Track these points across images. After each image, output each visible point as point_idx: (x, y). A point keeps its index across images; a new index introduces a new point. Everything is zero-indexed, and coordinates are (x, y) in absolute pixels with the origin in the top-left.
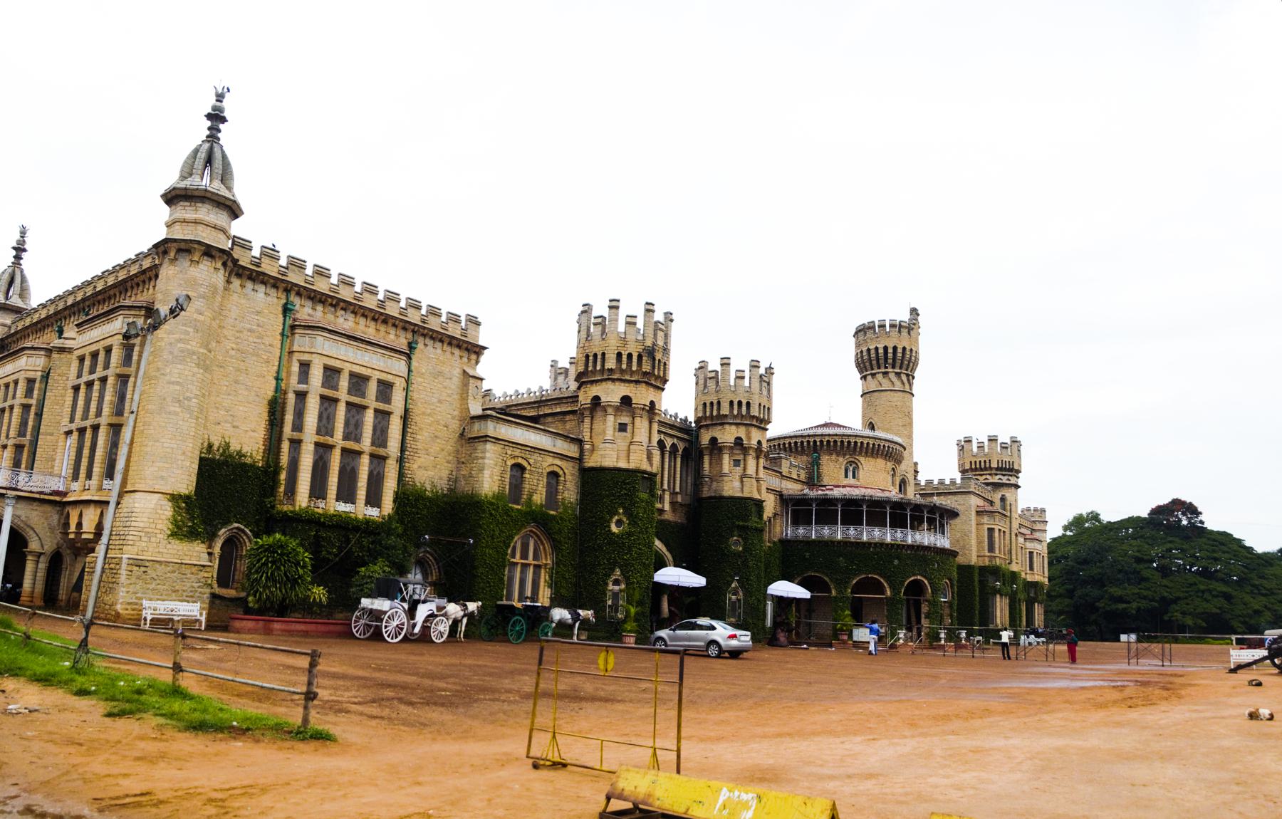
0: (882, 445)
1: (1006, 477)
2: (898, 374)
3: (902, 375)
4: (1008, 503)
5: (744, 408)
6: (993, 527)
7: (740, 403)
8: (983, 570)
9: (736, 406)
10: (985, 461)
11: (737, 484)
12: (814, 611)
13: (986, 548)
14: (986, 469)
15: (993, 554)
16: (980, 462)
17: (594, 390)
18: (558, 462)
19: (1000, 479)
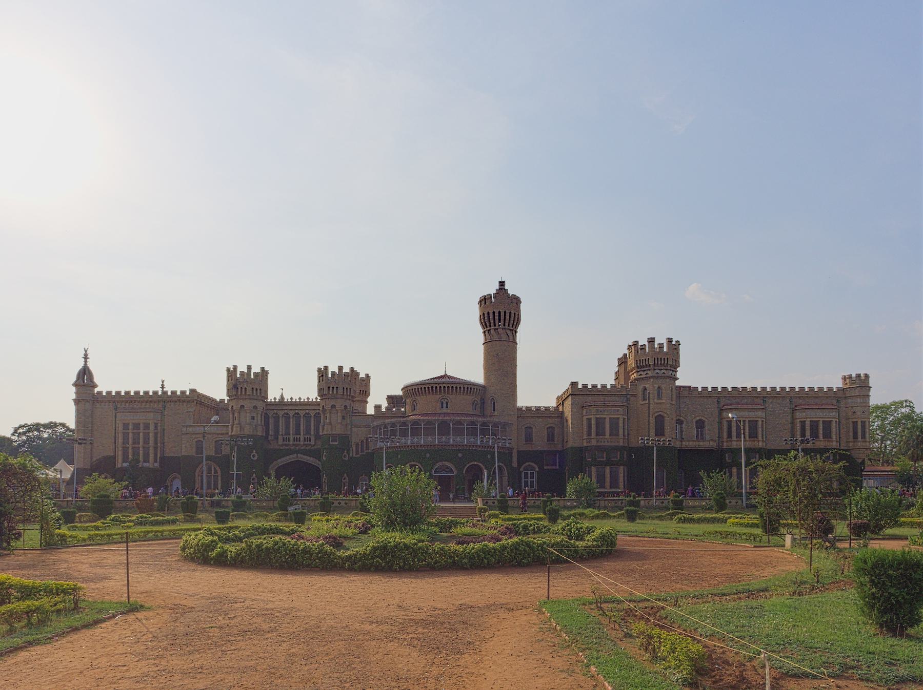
0: (426, 387)
1: (645, 372)
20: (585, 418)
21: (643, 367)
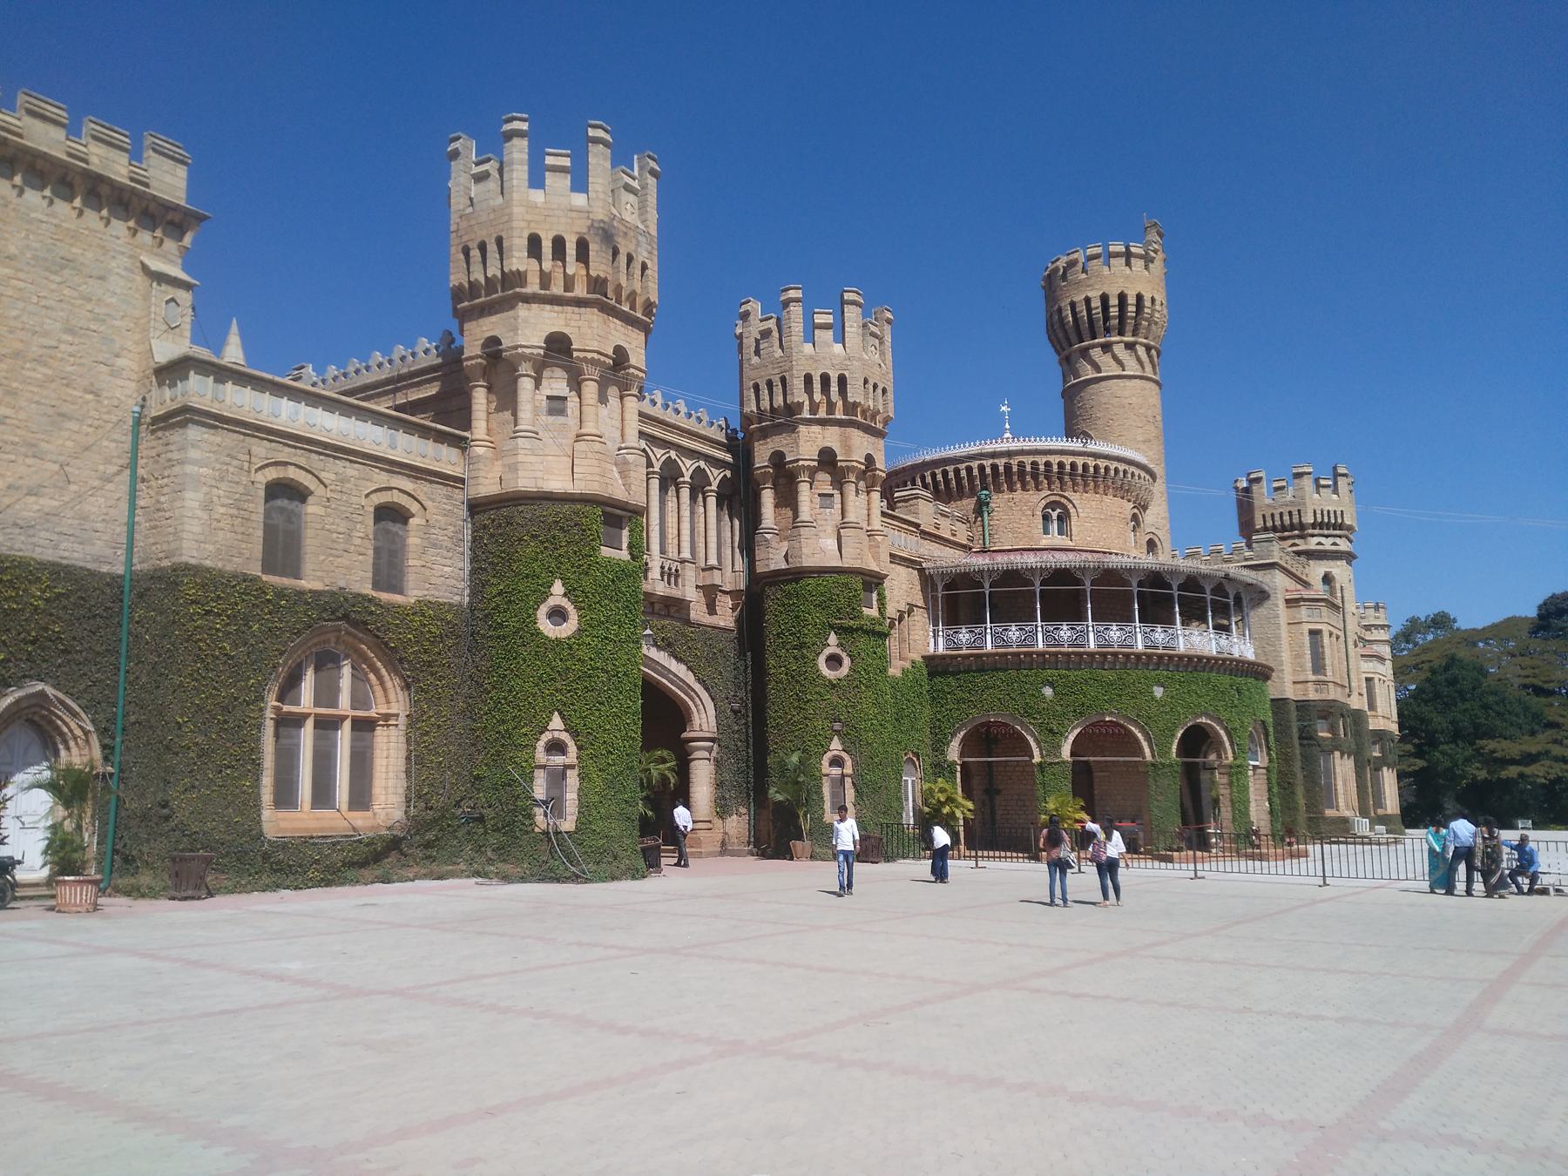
0: (1112, 467)
1: (1331, 540)
2: (1130, 346)
3: (1138, 347)
4: (1338, 586)
5: (834, 388)
6: (1318, 627)
7: (825, 379)
8: (1303, 706)
9: (817, 386)
10: (1290, 513)
11: (831, 543)
12: (998, 792)
13: (1309, 665)
14: (1292, 527)
15: (1322, 678)
16: (1281, 514)
17: (488, 326)
18: (408, 485)
19: (1319, 544)
20: (1306, 627)
21: (1328, 526)
